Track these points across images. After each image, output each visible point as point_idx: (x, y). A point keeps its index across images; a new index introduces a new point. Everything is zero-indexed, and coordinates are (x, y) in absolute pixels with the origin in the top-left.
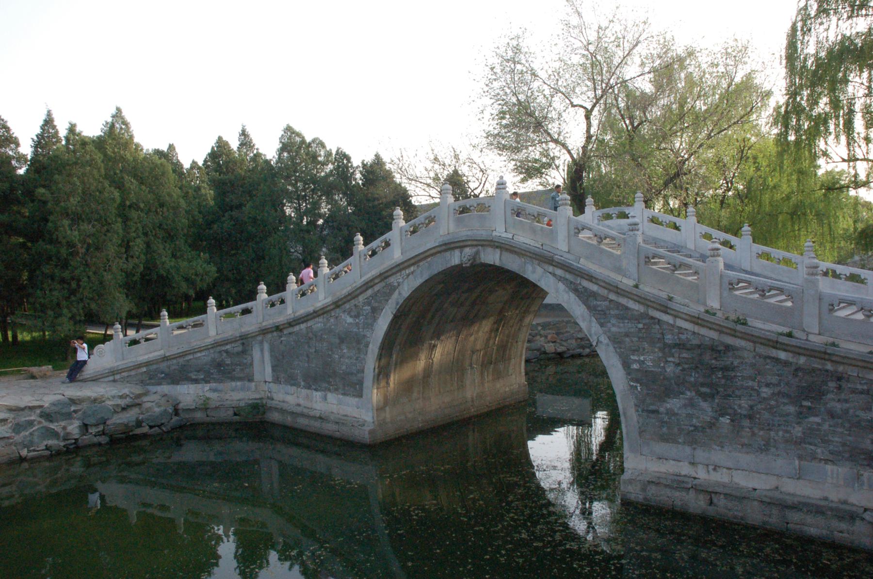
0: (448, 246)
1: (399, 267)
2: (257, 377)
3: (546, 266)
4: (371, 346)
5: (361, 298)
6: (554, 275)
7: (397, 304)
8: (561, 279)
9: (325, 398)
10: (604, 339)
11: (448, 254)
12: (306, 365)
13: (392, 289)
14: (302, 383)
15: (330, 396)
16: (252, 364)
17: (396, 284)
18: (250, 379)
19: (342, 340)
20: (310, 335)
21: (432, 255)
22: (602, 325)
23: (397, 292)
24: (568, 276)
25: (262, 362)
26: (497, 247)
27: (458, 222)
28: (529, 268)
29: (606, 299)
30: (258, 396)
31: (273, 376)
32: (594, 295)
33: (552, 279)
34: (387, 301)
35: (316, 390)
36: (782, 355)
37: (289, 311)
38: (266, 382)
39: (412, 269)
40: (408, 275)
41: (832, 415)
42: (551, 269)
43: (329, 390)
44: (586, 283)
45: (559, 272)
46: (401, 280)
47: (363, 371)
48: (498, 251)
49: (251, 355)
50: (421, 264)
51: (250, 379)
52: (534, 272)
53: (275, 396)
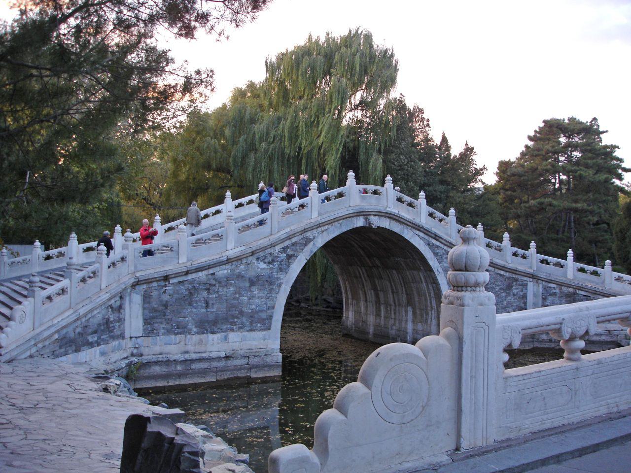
0: (358, 214)
1: (319, 226)
2: (127, 335)
3: (415, 231)
4: (283, 286)
5: (278, 248)
6: (419, 236)
7: (312, 252)
8: (422, 238)
9: (226, 338)
10: (441, 270)
11: (355, 219)
12: (204, 310)
13: (307, 241)
14: (195, 330)
15: (232, 336)
16: (124, 320)
17: (312, 237)
18: (122, 336)
19: (252, 283)
20: (213, 282)
21: (344, 219)
22: (440, 263)
23: (312, 243)
24: (426, 237)
25: (134, 318)
26: (389, 217)
27: (363, 199)
28: (406, 231)
29: (442, 249)
30: (125, 355)
31: (144, 330)
32: (437, 247)
33: (417, 238)
34: (302, 249)
35: (213, 333)
36: (502, 272)
37: (183, 259)
38: (131, 338)
39: (326, 227)
40: (322, 232)
41: (514, 295)
42: (417, 232)
43: (232, 330)
44: (434, 241)
45: (422, 234)
46: (316, 235)
47: (273, 307)
48: (388, 220)
49: (124, 309)
50: (334, 224)
51: (122, 336)
52: (408, 234)
53: (145, 351)
